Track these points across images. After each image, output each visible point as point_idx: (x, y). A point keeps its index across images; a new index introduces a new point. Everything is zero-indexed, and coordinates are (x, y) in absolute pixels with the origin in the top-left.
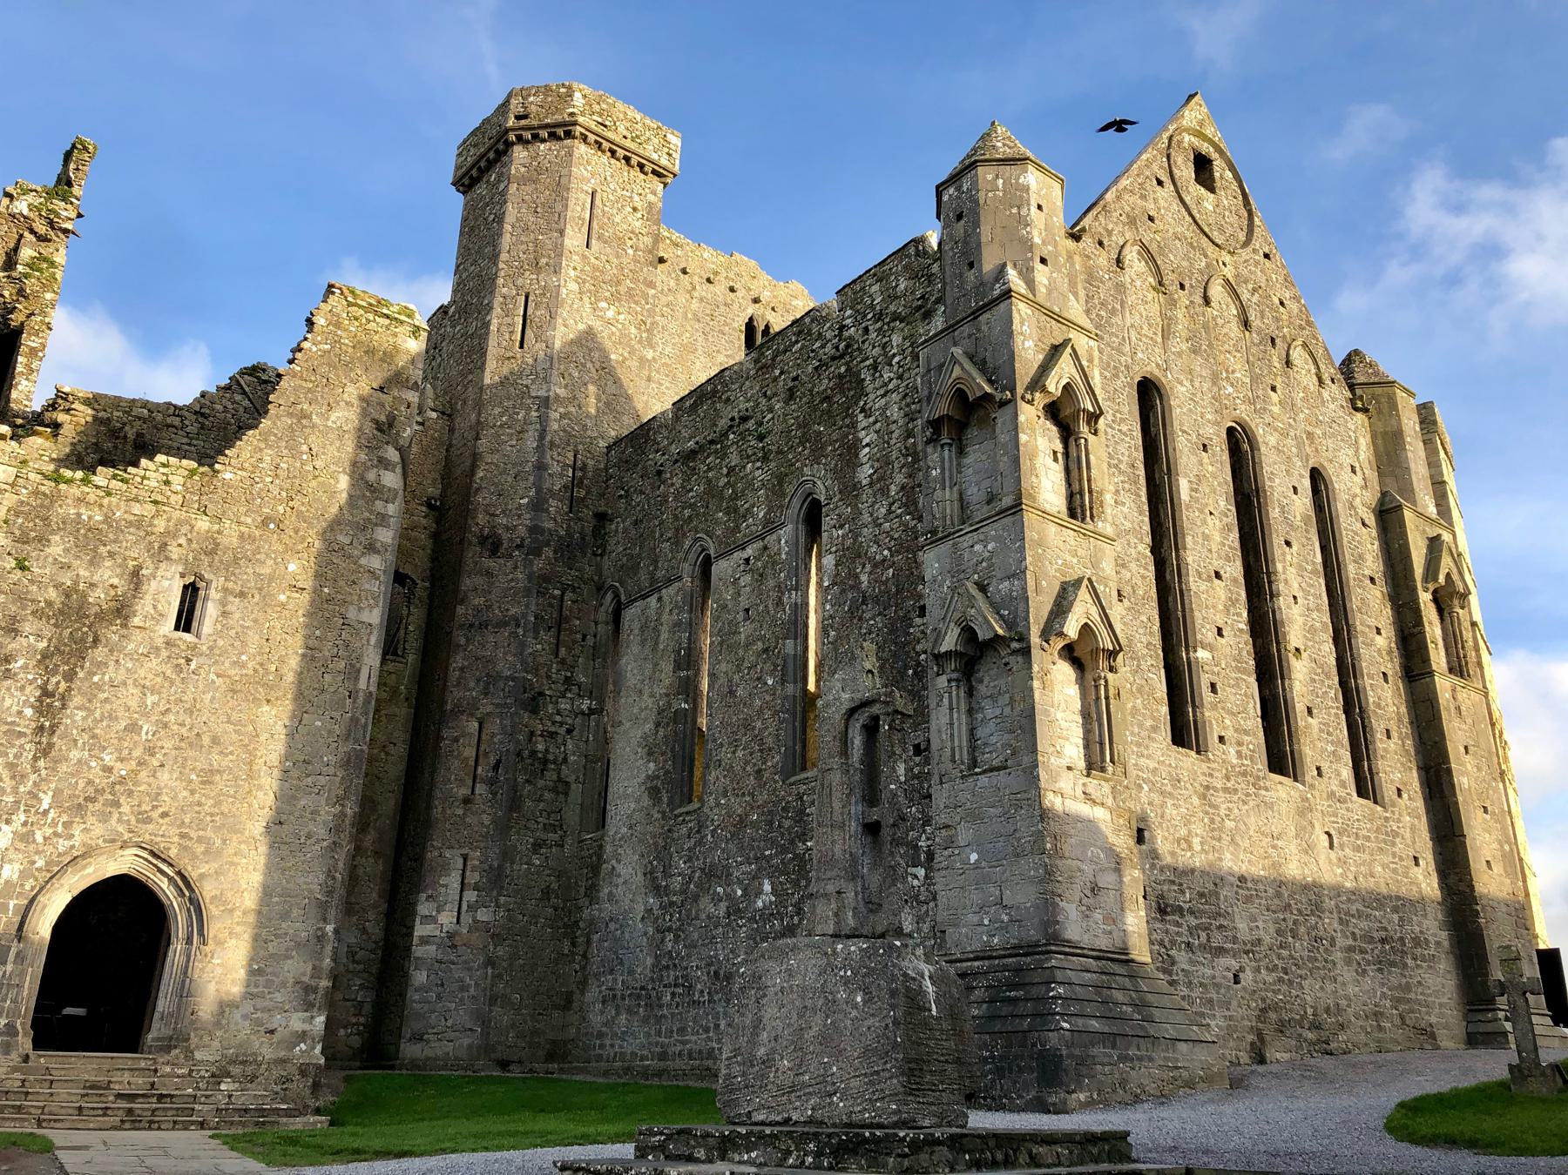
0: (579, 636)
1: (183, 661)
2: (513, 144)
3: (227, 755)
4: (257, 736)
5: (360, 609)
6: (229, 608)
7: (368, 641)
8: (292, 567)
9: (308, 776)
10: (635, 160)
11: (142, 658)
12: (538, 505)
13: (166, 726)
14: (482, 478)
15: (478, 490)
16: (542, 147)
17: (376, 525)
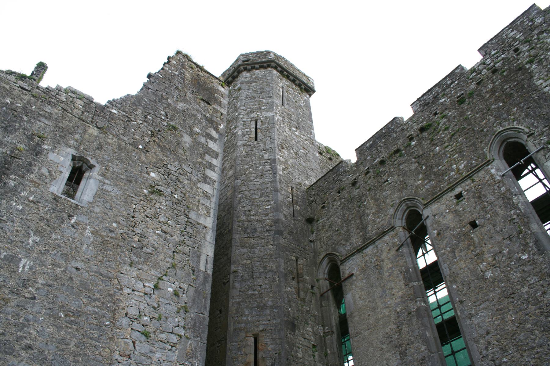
0: (310, 287)
1: (65, 215)
2: (242, 71)
3: (94, 300)
4: (121, 289)
5: (198, 215)
6: (105, 187)
7: (204, 237)
8: (153, 175)
9: (162, 332)
10: (297, 82)
11: (32, 205)
12: (277, 209)
13: (43, 264)
14: (240, 198)
15: (240, 203)
16: (257, 71)
17: (207, 167)
